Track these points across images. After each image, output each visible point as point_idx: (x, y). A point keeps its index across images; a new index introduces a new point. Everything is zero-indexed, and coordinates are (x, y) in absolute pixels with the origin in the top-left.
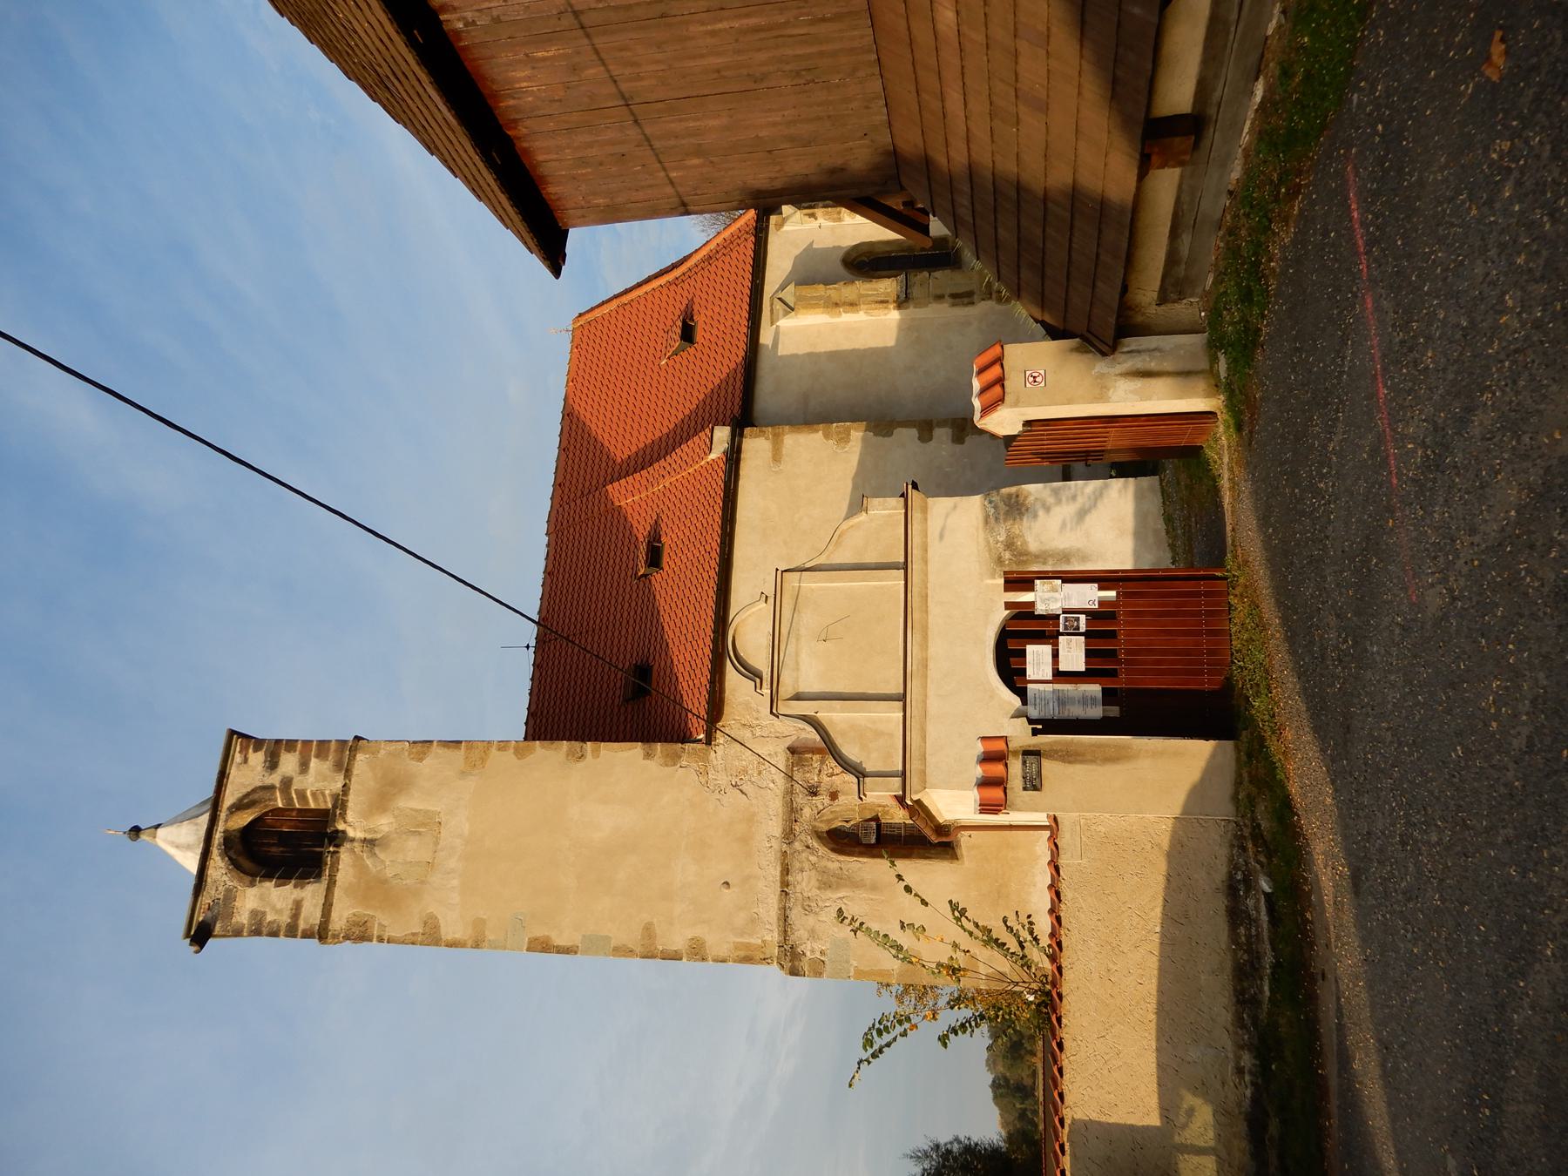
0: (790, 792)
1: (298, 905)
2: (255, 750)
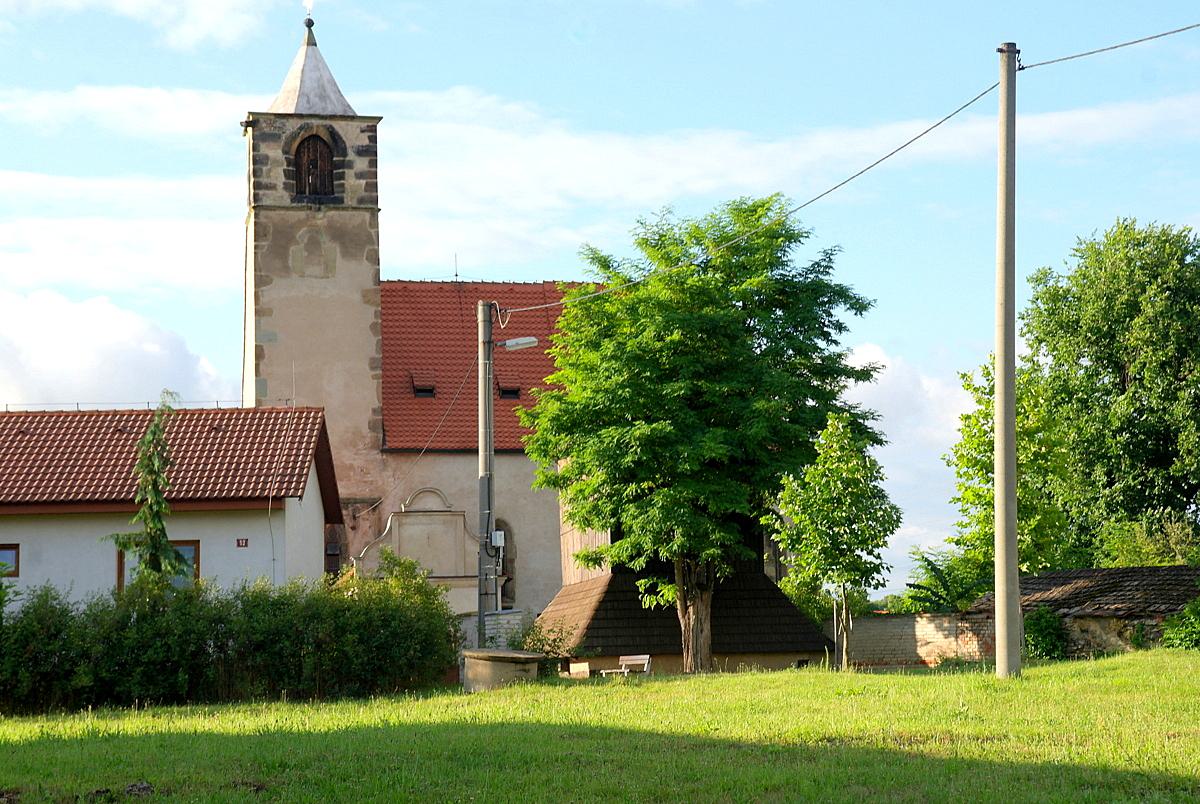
0: (356, 501)
1: (273, 187)
2: (369, 137)
